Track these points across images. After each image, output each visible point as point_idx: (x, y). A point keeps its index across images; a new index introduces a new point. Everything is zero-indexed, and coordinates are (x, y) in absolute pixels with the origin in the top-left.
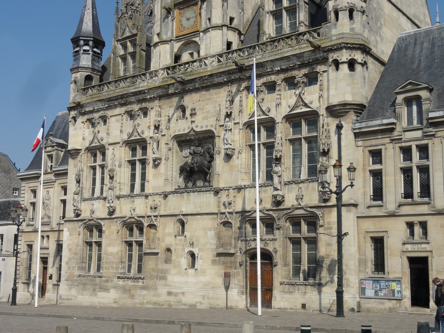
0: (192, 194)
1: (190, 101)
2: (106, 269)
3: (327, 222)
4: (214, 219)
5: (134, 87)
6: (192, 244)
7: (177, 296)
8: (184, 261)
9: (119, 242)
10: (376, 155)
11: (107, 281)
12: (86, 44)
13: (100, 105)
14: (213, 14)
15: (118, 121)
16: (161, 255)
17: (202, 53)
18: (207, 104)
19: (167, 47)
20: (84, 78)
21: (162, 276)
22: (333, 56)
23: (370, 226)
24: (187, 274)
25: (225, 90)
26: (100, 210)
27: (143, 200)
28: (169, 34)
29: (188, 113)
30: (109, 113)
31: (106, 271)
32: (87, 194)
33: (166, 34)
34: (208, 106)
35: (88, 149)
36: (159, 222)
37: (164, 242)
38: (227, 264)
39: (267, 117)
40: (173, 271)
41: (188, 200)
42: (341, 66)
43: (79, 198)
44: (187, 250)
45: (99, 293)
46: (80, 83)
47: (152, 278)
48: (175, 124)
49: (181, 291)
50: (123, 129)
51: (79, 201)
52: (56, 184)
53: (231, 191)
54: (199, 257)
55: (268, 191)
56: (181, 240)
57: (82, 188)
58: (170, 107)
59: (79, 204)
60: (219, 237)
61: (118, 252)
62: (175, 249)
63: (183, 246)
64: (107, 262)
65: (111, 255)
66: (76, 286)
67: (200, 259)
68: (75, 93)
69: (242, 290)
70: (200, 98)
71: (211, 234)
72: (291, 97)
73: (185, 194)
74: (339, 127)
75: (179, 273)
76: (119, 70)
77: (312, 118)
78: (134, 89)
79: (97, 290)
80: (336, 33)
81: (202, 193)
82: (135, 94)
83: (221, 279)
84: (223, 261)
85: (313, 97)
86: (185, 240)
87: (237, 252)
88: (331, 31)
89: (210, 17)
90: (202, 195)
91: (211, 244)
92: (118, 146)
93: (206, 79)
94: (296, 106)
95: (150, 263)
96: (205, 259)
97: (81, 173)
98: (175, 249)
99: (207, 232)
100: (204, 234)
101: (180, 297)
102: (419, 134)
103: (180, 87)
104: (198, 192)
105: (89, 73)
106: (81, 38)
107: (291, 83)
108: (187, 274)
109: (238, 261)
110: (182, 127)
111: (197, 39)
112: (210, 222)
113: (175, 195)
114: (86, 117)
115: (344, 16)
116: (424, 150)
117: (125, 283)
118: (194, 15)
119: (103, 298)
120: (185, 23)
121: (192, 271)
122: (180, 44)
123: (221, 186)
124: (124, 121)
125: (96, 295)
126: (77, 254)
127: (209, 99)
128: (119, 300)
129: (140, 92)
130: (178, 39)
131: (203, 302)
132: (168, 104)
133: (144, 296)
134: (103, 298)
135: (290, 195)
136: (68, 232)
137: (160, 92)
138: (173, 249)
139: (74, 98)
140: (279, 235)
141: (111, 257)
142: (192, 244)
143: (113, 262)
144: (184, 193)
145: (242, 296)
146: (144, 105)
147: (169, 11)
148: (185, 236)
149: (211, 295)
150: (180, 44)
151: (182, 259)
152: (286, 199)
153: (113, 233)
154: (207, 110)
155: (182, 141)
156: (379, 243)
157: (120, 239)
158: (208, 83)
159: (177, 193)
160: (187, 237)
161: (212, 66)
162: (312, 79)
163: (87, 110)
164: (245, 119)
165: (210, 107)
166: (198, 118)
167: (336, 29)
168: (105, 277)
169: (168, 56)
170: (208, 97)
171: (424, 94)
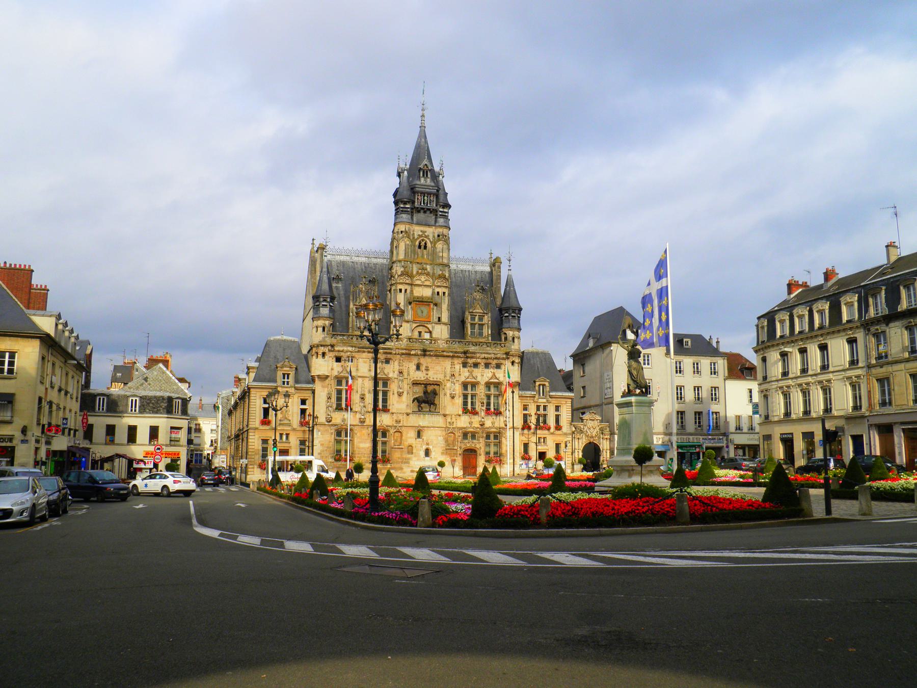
1: (425, 361)
6: (428, 444)
10: (525, 408)
12: (325, 301)
13: (350, 349)
19: (408, 325)
21: (407, 461)
22: (512, 359)
23: (525, 439)
26: (350, 419)
29: (423, 368)
30: (356, 355)
35: (336, 377)
36: (404, 430)
40: (414, 459)
44: (424, 447)
47: (397, 462)
52: (296, 396)
60: (447, 441)
74: (513, 392)
77: (498, 385)
85: (500, 375)
100: (436, 439)
102: (544, 400)
103: (419, 352)
107: (487, 366)
110: (420, 376)
111: (429, 326)
114: (332, 354)
115: (516, 340)
116: (545, 408)
120: (419, 312)
121: (427, 458)
122: (415, 325)
130: (414, 321)
137: (404, 351)
139: (324, 338)
142: (428, 444)
146: (389, 356)
147: (410, 303)
150: (415, 325)
154: (437, 370)
155: (415, 383)
156: (526, 446)
158: (439, 355)
161: (442, 345)
162: (498, 366)
163: (336, 349)
164: (463, 379)
165: (438, 368)
166: (431, 373)
171: (547, 384)
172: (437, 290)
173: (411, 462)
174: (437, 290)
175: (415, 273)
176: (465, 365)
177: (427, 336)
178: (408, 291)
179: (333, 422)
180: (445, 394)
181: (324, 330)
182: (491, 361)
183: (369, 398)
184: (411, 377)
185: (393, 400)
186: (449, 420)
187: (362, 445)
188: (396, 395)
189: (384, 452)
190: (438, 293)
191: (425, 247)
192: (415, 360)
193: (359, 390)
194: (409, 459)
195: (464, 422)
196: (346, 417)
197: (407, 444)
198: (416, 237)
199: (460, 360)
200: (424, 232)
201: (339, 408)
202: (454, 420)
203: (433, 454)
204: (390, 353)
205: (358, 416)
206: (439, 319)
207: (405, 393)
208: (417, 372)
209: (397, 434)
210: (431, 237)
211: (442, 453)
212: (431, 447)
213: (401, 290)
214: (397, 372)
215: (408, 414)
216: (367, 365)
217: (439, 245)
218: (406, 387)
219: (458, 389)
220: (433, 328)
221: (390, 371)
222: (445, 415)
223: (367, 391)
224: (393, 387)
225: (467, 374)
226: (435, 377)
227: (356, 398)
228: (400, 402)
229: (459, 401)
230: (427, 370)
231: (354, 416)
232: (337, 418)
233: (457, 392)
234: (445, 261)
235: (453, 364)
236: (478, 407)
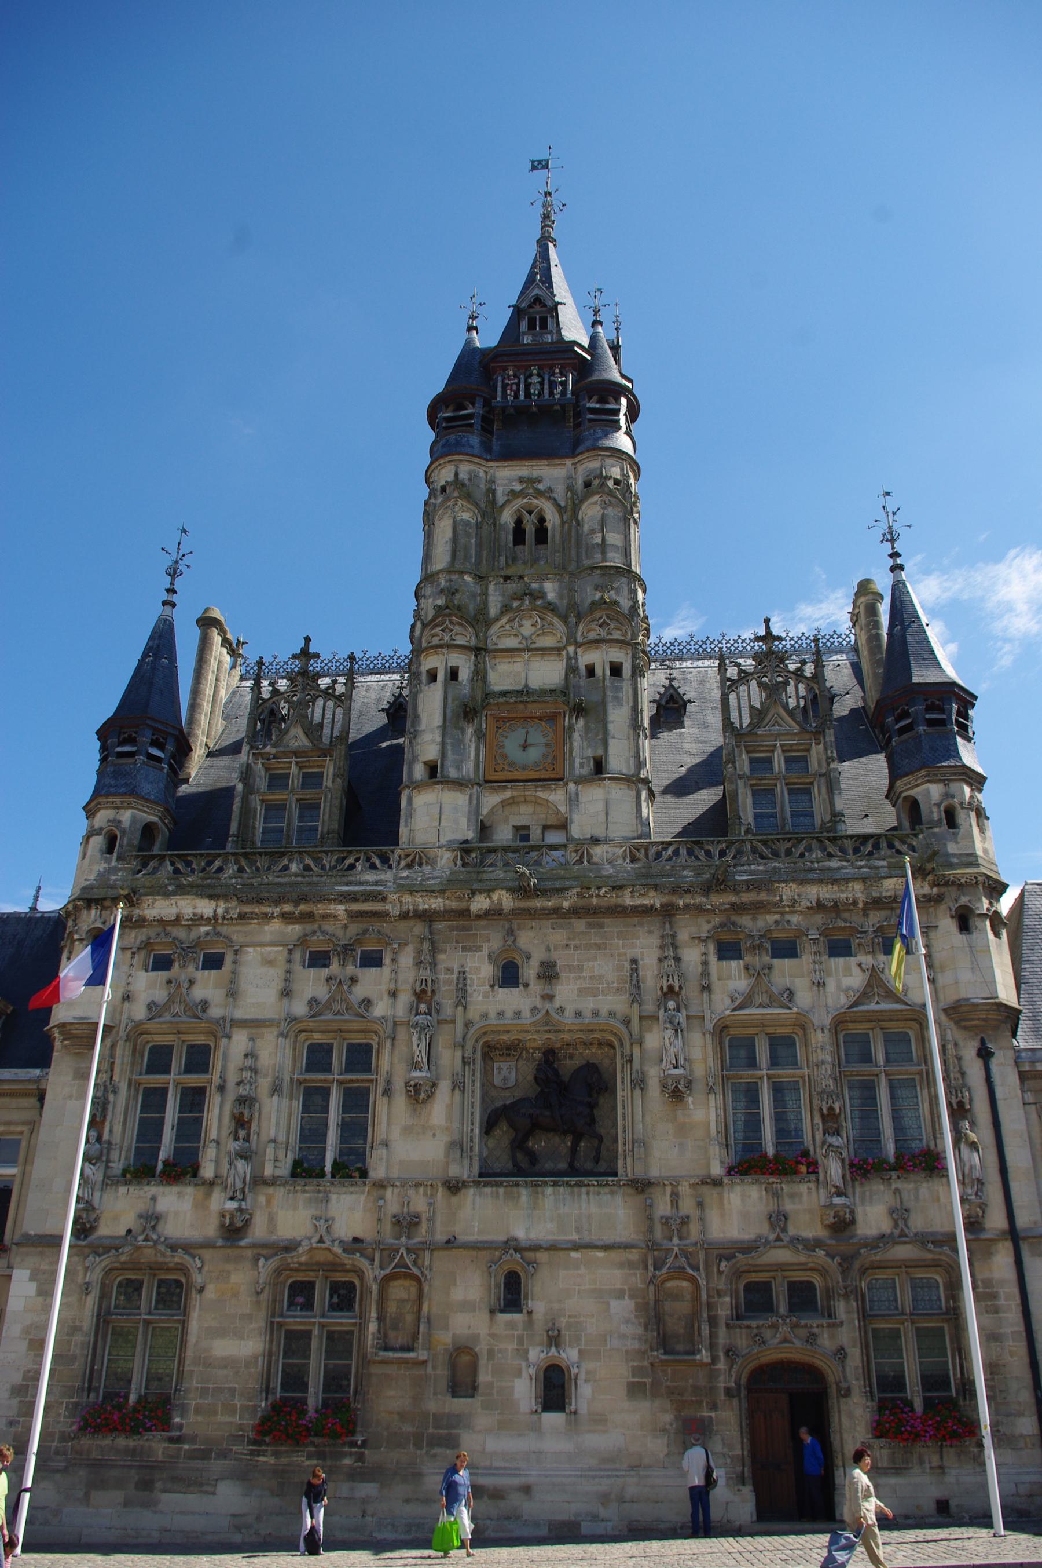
0: (549, 1190)
1: (535, 942)
2: (198, 1411)
3: (983, 1281)
4: (630, 1265)
5: (345, 879)
6: (554, 1339)
7: (502, 1498)
8: (524, 1391)
9: (260, 1323)
11: (204, 1455)
14: (612, 750)
15: (270, 963)
16: (434, 1368)
17: (576, 831)
18: (595, 959)
20: (139, 826)
24: (536, 1428)
25: (650, 932)
27: (363, 1198)
28: (469, 768)
29: (530, 971)
31: (200, 1419)
32: (277, 1163)
33: (458, 768)
34: (596, 963)
37: (446, 1328)
38: (681, 1394)
39: (788, 1011)
40: (483, 1420)
41: (535, 1207)
42: (978, 922)
43: (100, 1177)
44: (536, 1354)
45: (165, 1497)
46: (130, 840)
48: (486, 996)
49: (516, 1481)
50: (296, 987)
51: (98, 1186)
53: (684, 1189)
54: (582, 1376)
55: (801, 1195)
56: (511, 1325)
57: (109, 1143)
58: (464, 949)
59: (97, 1194)
61: (256, 1358)
62: (491, 1353)
63: (520, 1340)
64: (204, 1392)
65: (226, 1367)
66: (58, 1471)
67: (586, 1381)
68: (109, 861)
69: (739, 1469)
70: (569, 939)
71: (623, 1308)
72: (848, 972)
73: (524, 1193)
75: (503, 1426)
76: (254, 828)
78: (347, 884)
79: (159, 1485)
80: (957, 852)
81: (584, 1190)
82: (353, 898)
83: (665, 1441)
84: (668, 1387)
86: (530, 1323)
87: (714, 1359)
88: (945, 844)
89: (600, 752)
90: (584, 1197)
91: (624, 1336)
92: (275, 1031)
93: (598, 896)
94: (864, 996)
95: (392, 1393)
96: (602, 1383)
97: (111, 1097)
98: (491, 1353)
99: (608, 1303)
101: (516, 1500)
104: (570, 1185)
105: (154, 819)
106: (149, 722)
108: (536, 1428)
109: (722, 1385)
112: (617, 1272)
113: (488, 1190)
117: (284, 1460)
118: (544, 741)
119: (182, 1513)
123: (654, 1173)
124: (297, 967)
125: (149, 1504)
126: (74, 1358)
127: (598, 947)
128: (259, 1518)
129: (369, 897)
131: (603, 1513)
132: (457, 942)
133: (365, 1501)
134: (182, 1513)
135: (868, 1208)
136: (34, 1286)
138: (482, 1348)
140: (848, 1312)
141: (225, 1372)
142: (554, 1339)
143: (232, 1391)
144: (517, 1185)
145: (741, 1487)
148: (530, 1313)
149: (631, 1491)
151: (516, 1380)
152: (859, 1218)
153: (235, 1295)
157: (263, 1314)
159: (492, 1186)
160: (535, 1316)
166: (566, 992)
167: (957, 843)
168: (193, 1439)
169: (463, 822)
170: (595, 940)
172: (586, 658)
173: (470, 1442)
174: (586, 658)
175: (493, 611)
176: (728, 950)
177: (554, 838)
178: (464, 675)
179: (105, 1230)
180: (640, 1083)
181: (110, 850)
182: (856, 919)
183: (278, 1119)
184: (473, 1013)
185: (390, 1117)
186: (663, 1207)
187: (223, 1348)
188: (400, 1101)
189: (335, 1380)
190: (591, 671)
191: (542, 535)
192: (493, 940)
193: (232, 1078)
194: (456, 1421)
195: (738, 1213)
196: (162, 1206)
197: (444, 1339)
198: (501, 499)
199: (704, 927)
200: (531, 481)
201: (142, 1170)
202: (687, 1206)
203: (584, 1395)
204: (383, 915)
205: (219, 1202)
206: (599, 767)
207: (444, 1087)
208: (502, 993)
209: (400, 1290)
210: (560, 493)
211: (634, 1390)
212: (569, 1355)
213: (433, 677)
214: (405, 998)
215: (454, 1187)
216: (274, 976)
217: (591, 511)
218: (448, 1058)
219: (701, 1053)
220: (573, 801)
221: (382, 992)
222: (642, 1186)
223: (264, 1084)
224: (390, 1062)
225: (741, 984)
226: (588, 1005)
227: (216, 1116)
228: (419, 1138)
229: (706, 1112)
230: (549, 973)
231: (201, 1206)
232: (122, 1210)
233: (699, 1071)
234: (616, 560)
235: (670, 945)
236: (810, 1131)
